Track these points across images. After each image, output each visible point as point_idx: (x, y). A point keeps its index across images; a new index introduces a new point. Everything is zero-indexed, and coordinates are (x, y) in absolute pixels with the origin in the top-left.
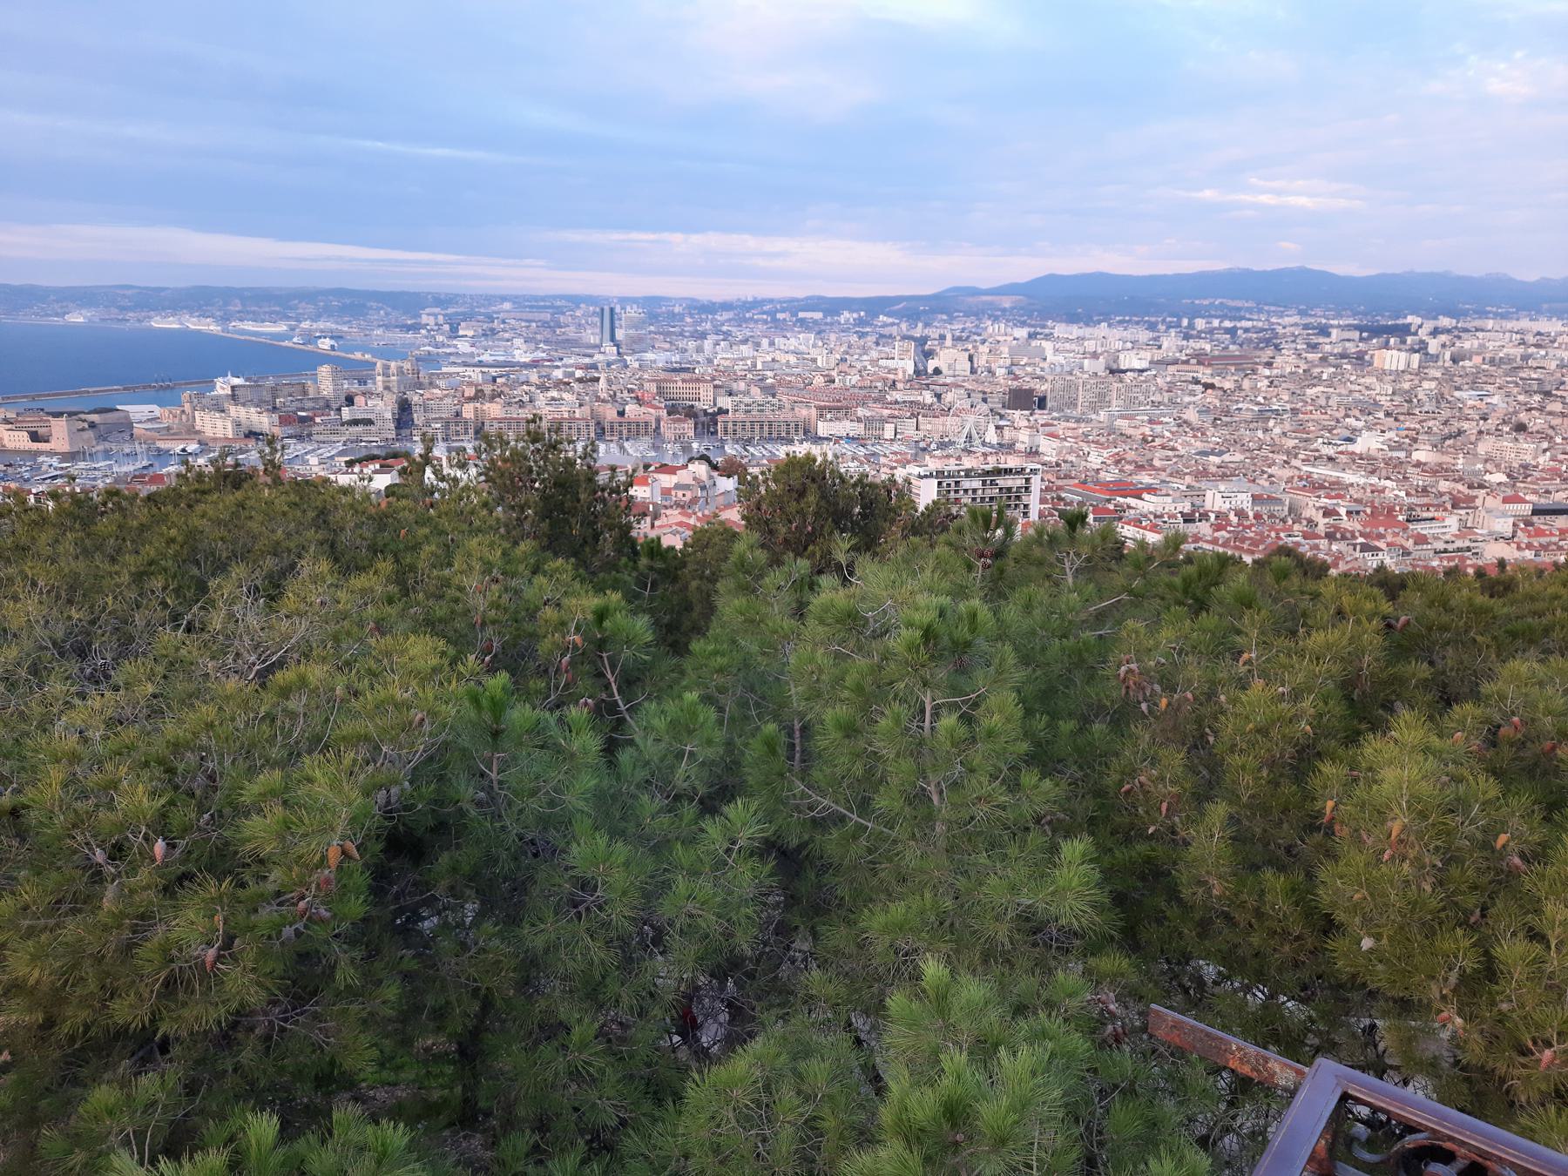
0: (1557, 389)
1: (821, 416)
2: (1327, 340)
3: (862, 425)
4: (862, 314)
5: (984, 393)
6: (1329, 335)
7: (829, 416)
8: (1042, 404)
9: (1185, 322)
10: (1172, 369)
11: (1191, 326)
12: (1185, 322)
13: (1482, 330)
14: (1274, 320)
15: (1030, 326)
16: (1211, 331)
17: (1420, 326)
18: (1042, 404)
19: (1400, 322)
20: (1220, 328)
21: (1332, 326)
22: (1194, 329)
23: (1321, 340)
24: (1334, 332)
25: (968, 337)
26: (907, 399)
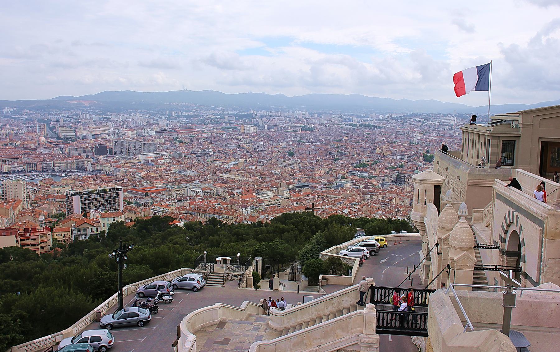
0: (302, 139)
1: (3, 162)
2: (223, 121)
3: (26, 166)
4: (15, 109)
5: (84, 148)
6: (224, 118)
7: (7, 163)
8: (111, 152)
9: (168, 113)
10: (164, 135)
11: (170, 114)
12: (168, 113)
13: (277, 116)
14: (203, 112)
15: (99, 114)
16: (178, 116)
17: (256, 115)
18: (111, 152)
19: (249, 113)
20: (182, 115)
21: (225, 115)
22: (172, 116)
23: (221, 120)
24: (226, 117)
25: (71, 120)
26: (46, 152)
